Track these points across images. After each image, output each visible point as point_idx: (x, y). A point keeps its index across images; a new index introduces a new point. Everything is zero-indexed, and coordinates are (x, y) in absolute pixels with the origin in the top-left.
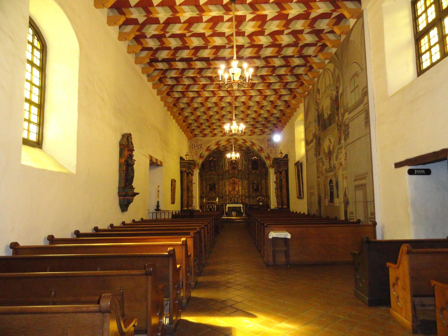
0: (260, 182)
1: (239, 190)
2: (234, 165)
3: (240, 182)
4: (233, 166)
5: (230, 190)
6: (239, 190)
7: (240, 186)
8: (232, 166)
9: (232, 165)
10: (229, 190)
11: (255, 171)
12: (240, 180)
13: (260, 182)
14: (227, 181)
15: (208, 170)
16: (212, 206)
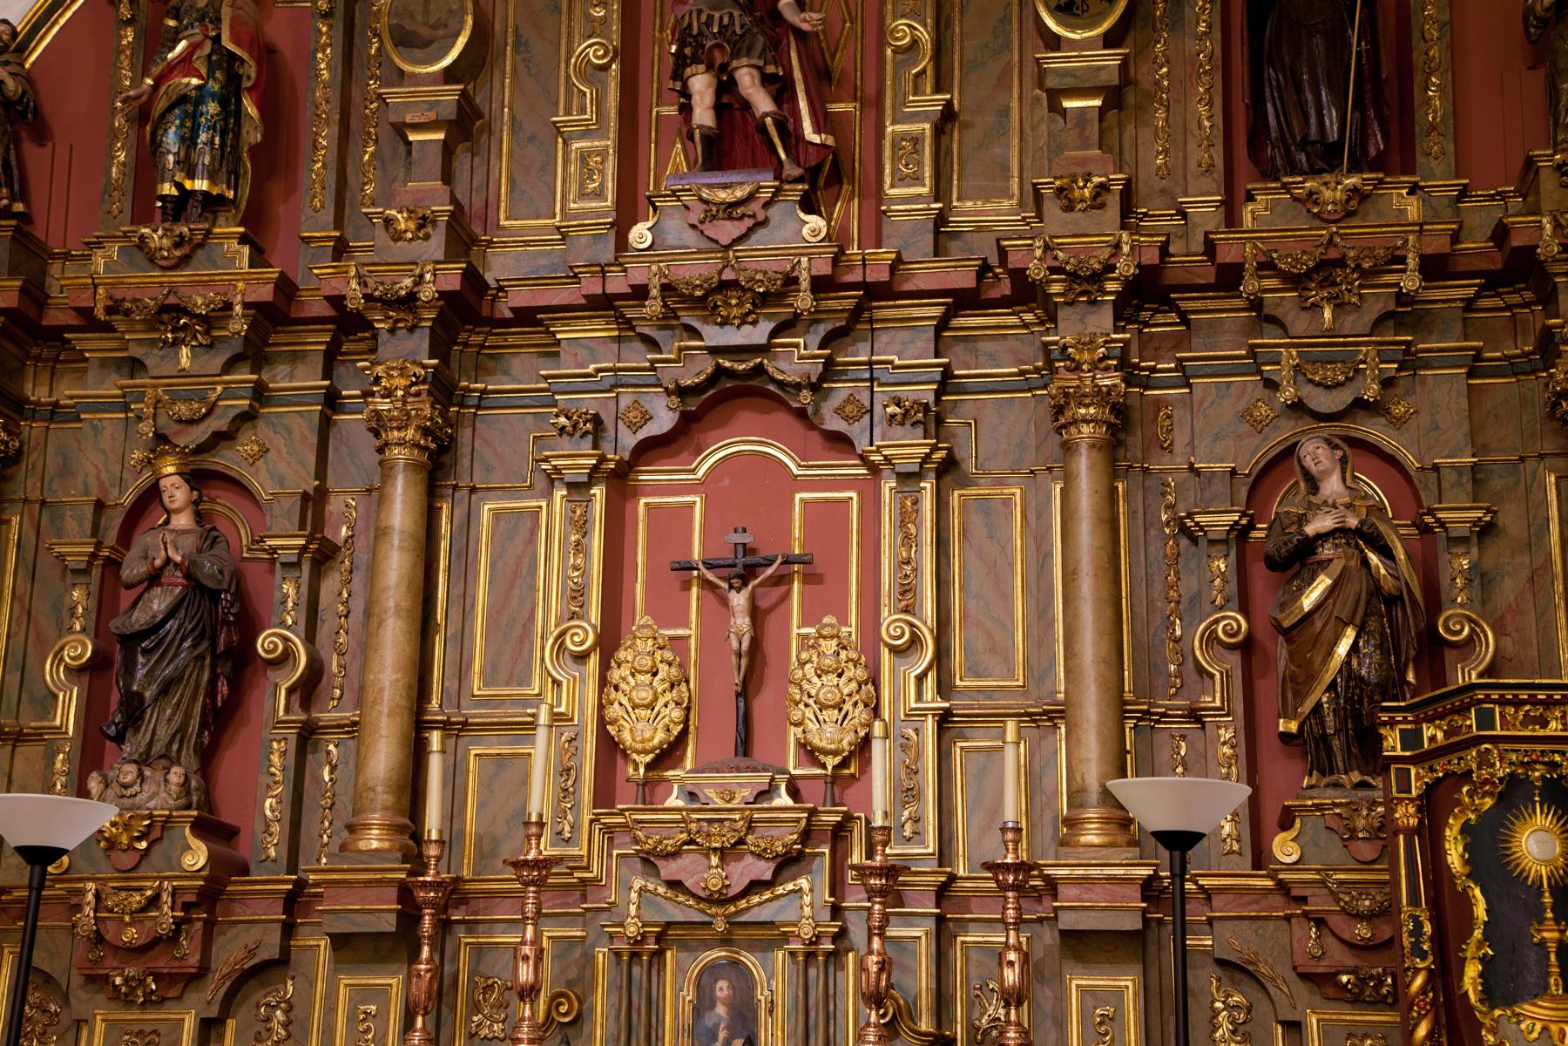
0: (1460, 516)
2: (747, 81)
3: (906, 518)
4: (727, 96)
7: (892, 625)
8: (703, 115)
9: (701, 85)
10: (610, 749)
11: (1334, 189)
13: (1460, 516)
14: (578, 488)
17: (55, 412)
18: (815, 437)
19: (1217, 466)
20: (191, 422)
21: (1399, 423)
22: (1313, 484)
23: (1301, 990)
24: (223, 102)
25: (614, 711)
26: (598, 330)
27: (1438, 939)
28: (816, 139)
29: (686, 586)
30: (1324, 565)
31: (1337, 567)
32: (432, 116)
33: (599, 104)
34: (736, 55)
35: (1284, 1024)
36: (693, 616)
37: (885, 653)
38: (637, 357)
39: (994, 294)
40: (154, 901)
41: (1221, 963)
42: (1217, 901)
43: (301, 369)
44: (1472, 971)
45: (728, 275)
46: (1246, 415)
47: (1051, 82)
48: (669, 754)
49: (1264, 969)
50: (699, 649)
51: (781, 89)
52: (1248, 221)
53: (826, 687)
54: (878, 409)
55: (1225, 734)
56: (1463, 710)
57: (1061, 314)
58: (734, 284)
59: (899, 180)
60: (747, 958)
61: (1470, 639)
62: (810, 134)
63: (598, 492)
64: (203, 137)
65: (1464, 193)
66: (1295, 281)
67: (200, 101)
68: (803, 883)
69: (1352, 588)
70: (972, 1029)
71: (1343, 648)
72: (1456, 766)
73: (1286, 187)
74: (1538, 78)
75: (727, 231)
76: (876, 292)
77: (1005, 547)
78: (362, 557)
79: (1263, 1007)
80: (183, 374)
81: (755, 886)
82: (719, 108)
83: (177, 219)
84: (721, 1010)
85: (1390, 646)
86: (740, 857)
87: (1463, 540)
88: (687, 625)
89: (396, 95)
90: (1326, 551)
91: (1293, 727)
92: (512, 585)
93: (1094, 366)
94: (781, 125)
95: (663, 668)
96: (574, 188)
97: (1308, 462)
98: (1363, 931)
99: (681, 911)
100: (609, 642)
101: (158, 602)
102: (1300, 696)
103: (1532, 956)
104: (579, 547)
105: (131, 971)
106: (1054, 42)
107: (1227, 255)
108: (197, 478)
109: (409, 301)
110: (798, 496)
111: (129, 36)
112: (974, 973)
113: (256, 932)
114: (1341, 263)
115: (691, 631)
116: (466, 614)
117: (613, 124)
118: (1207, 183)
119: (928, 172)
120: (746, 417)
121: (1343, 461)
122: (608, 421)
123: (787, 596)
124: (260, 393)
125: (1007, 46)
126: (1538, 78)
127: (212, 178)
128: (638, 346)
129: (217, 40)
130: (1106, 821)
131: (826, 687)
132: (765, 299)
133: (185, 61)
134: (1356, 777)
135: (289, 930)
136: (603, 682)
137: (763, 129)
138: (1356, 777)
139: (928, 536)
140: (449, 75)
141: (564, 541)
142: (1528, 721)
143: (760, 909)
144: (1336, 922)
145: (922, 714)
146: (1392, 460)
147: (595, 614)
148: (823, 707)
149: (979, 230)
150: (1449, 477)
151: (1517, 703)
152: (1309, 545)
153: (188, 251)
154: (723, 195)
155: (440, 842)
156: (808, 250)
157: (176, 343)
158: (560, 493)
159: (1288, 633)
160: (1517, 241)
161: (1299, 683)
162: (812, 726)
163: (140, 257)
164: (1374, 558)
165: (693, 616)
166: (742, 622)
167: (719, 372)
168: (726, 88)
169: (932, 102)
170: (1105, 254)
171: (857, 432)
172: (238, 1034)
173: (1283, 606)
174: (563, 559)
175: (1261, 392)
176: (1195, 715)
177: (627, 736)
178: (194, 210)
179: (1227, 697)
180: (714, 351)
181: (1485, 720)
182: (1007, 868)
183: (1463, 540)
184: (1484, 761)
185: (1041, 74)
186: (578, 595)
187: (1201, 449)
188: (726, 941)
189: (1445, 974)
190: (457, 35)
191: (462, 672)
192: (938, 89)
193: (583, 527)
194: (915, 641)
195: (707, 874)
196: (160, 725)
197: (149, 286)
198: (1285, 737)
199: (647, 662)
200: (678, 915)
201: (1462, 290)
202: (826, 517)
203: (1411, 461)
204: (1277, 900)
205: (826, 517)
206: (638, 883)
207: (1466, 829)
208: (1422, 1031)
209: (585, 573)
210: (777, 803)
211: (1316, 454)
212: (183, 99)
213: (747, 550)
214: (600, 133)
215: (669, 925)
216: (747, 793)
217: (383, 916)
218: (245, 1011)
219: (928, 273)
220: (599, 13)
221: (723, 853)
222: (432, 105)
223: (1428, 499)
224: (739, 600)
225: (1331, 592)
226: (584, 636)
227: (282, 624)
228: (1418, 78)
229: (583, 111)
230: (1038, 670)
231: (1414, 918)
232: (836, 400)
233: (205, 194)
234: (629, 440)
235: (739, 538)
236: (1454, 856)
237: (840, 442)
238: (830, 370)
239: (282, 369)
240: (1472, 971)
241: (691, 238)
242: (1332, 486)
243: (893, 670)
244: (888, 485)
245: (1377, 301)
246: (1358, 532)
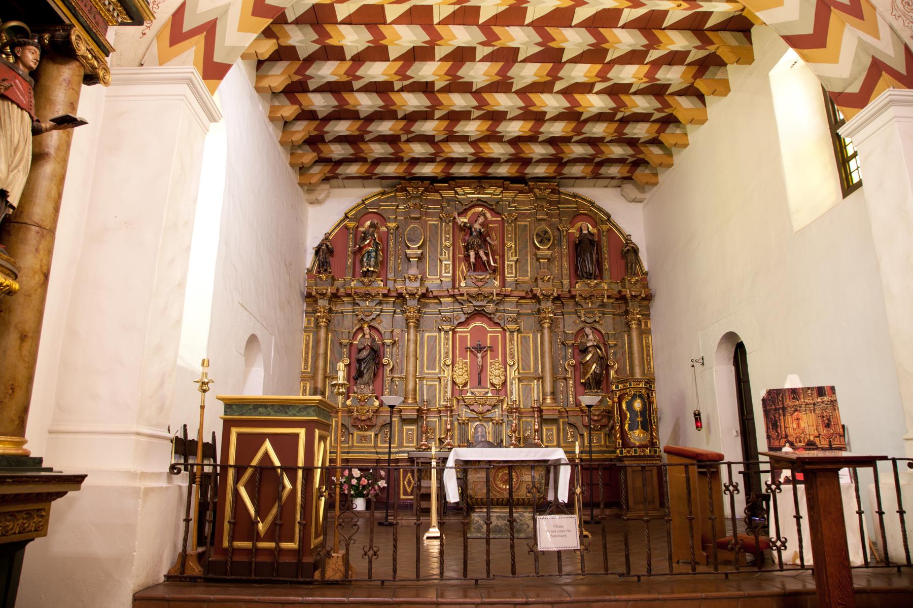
0: (612, 343)
1: (504, 384)
2: (481, 253)
3: (511, 340)
4: (477, 256)
5: (459, 380)
6: (504, 384)
7: (510, 362)
8: (472, 260)
9: (472, 253)
10: (454, 383)
12: (512, 332)
14: (446, 332)
15: (349, 278)
16: (286, 445)
17: (337, 312)
18: (491, 323)
19: (570, 332)
20: (368, 316)
21: (601, 325)
22: (587, 336)
23: (584, 429)
24: (376, 252)
25: (454, 376)
26: (450, 300)
27: (621, 420)
28: (493, 265)
29: (467, 351)
30: (590, 352)
31: (593, 352)
32: (415, 256)
33: (449, 254)
34: (480, 249)
35: (580, 434)
36: (469, 357)
37: (508, 366)
38: (457, 306)
39: (528, 297)
40: (368, 411)
41: (569, 424)
42: (569, 413)
43: (388, 305)
44: (627, 426)
45: (480, 292)
46: (574, 322)
47: (538, 256)
48: (465, 385)
49: (577, 425)
50: (470, 362)
51: (487, 255)
52: (577, 287)
53: (496, 372)
54: (506, 319)
55: (571, 382)
56: (626, 383)
57: (542, 302)
58: (481, 294)
59: (509, 273)
60: (484, 424)
61: (613, 366)
62: (492, 264)
63: (450, 333)
64: (372, 259)
65: (611, 282)
66: (585, 298)
67: (371, 252)
68: (497, 410)
69: (596, 356)
70: (524, 436)
71: (594, 367)
72: (625, 391)
73: (584, 281)
74: (623, 262)
75: (480, 284)
76: (506, 296)
77: (529, 346)
78: (401, 344)
79: (576, 431)
80: (367, 306)
81: (488, 410)
82: (475, 258)
83: (365, 276)
84: (479, 433)
85: (601, 367)
86: (485, 405)
87: (612, 347)
88: (467, 359)
89: (408, 251)
90: (590, 349)
91: (584, 381)
92: (431, 351)
93: (549, 312)
94: (488, 262)
95: (464, 368)
96: (443, 271)
97: (587, 332)
98: (596, 418)
99: (474, 415)
100: (453, 364)
101: (365, 353)
102: (585, 375)
103: (636, 423)
104: (447, 344)
105: (362, 425)
106: (538, 249)
107: (573, 293)
108: (370, 327)
109: (414, 295)
110: (489, 334)
111: (351, 235)
112: (524, 426)
113: (385, 418)
114: (593, 296)
115: (468, 361)
116: (423, 356)
117: (451, 258)
118: (566, 277)
119: (514, 272)
120: (478, 318)
121: (593, 332)
122: (452, 319)
123: (487, 354)
124: (381, 311)
125: (527, 247)
126: (623, 262)
127: (374, 267)
128: (457, 303)
129: (375, 240)
130: (551, 399)
131: (496, 372)
132: (485, 297)
133: (369, 245)
134: (596, 390)
135: (391, 417)
136: (453, 370)
137: (484, 263)
138: (596, 390)
139: (516, 344)
140: (419, 248)
141: (444, 343)
142: (637, 384)
143: (489, 415)
145: (515, 378)
146: (600, 332)
147: (451, 357)
148: (496, 376)
149: (523, 283)
150: (610, 335)
151: (635, 382)
152: (587, 348)
153: (371, 283)
154: (480, 277)
155: (427, 402)
156: (496, 289)
157: (367, 300)
158: (443, 333)
159: (583, 364)
160: (623, 294)
161: (585, 373)
162: (494, 380)
163: (361, 284)
164: (598, 350)
165: (469, 357)
166: (480, 359)
167: (475, 309)
168: (477, 254)
169: (515, 258)
170: (551, 292)
171: (501, 322)
172: (381, 437)
173: (582, 359)
174: (444, 346)
175: (577, 318)
176: (565, 379)
177: (457, 381)
178: (370, 274)
179: (572, 376)
180: (474, 306)
181: (630, 385)
182: (535, 408)
183: (612, 347)
184: (630, 391)
185: (536, 255)
186: (447, 353)
187: (566, 328)
188: (480, 421)
189: (622, 427)
190: (421, 240)
191: (422, 367)
192: (516, 256)
193: (448, 339)
195: (480, 409)
196: (366, 377)
197: (362, 289)
198: (582, 383)
199: (461, 367)
200: (472, 416)
201: (612, 300)
202: (494, 339)
203: (603, 332)
204: (580, 412)
205: (494, 339)
206: (465, 410)
207: (626, 402)
208: (618, 435)
209: (448, 349)
210: (489, 395)
211: (588, 330)
212: (369, 252)
213: (480, 345)
214: (449, 260)
215: (470, 418)
216: (484, 393)
217: (414, 415)
218: (382, 432)
219: (516, 293)
220: (448, 236)
221: (482, 405)
222: (416, 254)
223: (606, 339)
224: (479, 355)
225: (592, 357)
226: (449, 362)
227: (387, 357)
228: (603, 260)
229: (445, 256)
230: (536, 370)
231: (617, 417)
232: (497, 316)
233: (373, 271)
234: (456, 323)
235: (478, 343)
236: (624, 406)
237: (498, 324)
238: (497, 310)
239: (385, 305)
240: (627, 426)
241: (473, 285)
242: (591, 337)
243: (510, 370)
244: (508, 334)
246: (596, 346)
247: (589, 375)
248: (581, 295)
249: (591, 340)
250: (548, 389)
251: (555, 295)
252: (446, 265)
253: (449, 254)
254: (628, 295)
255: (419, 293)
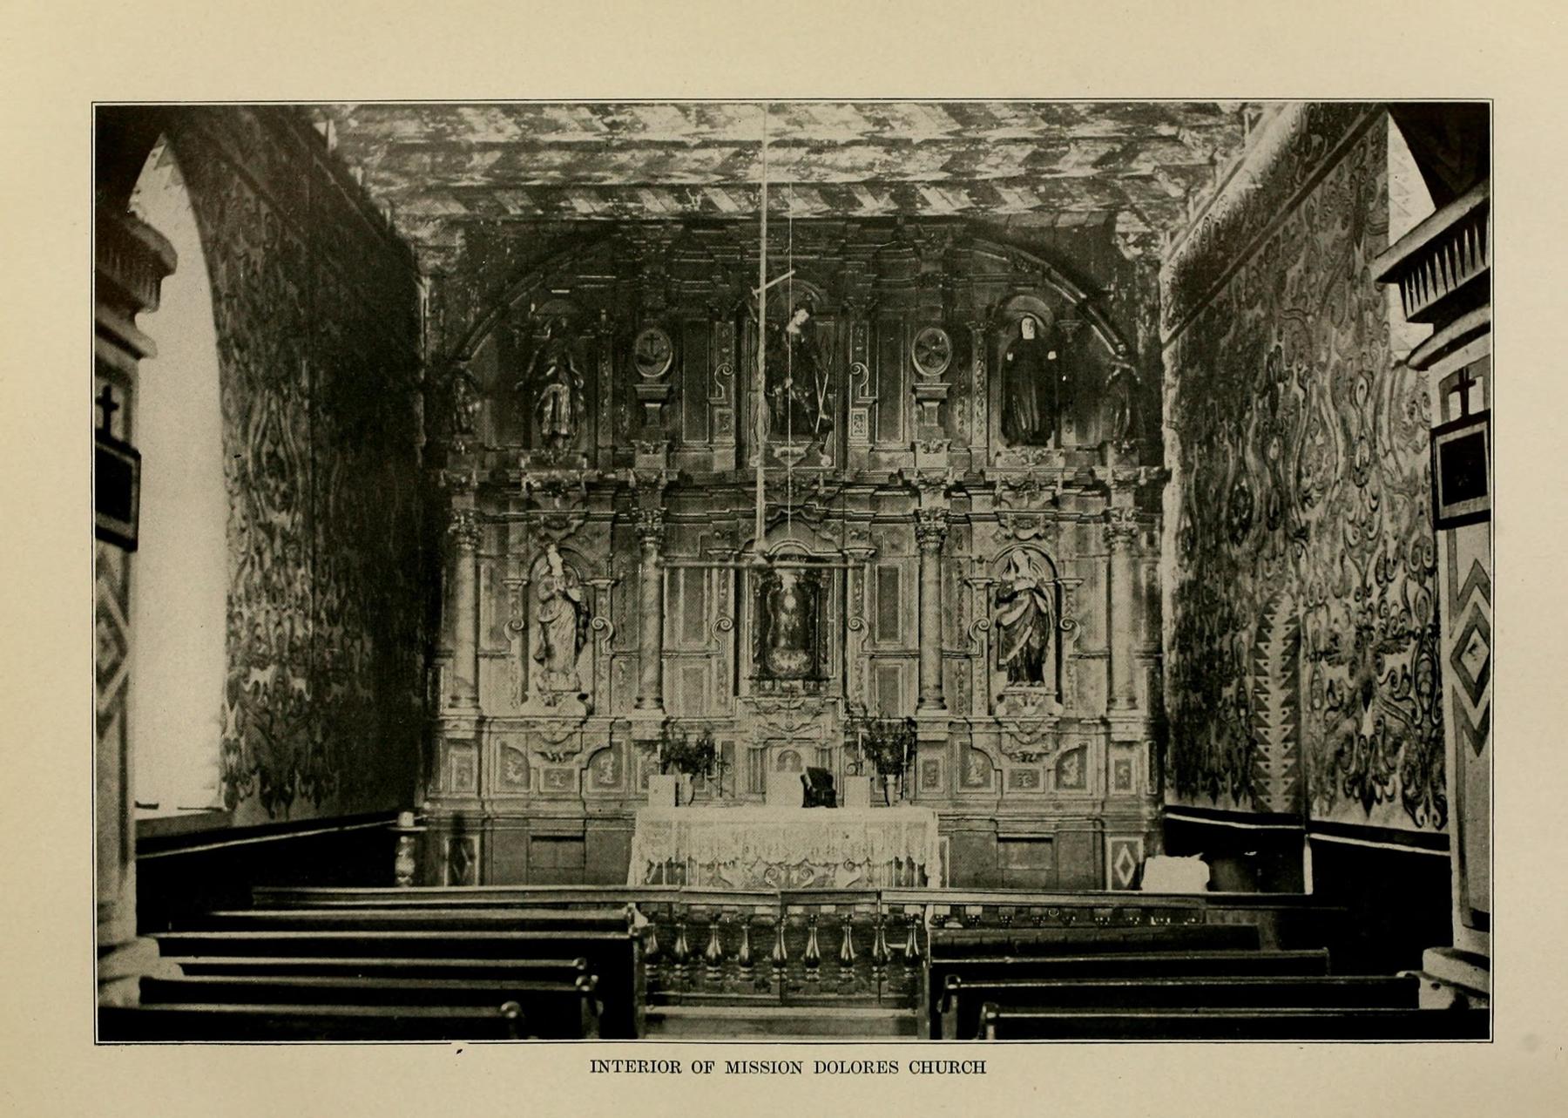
33: (727, 392)
102: (1008, 651)
104: (725, 586)
106: (920, 377)
140: (662, 379)
144: (1019, 736)
152: (1015, 594)
194: (862, 627)
214: (728, 406)
220: (725, 350)
229: (720, 395)
245: (1047, 496)
247: (1015, 652)
248: (1005, 483)
249: (1025, 578)
250: (931, 680)
251: (950, 482)
252: (721, 415)
253: (727, 392)
254: (1109, 481)
255: (664, 481)
